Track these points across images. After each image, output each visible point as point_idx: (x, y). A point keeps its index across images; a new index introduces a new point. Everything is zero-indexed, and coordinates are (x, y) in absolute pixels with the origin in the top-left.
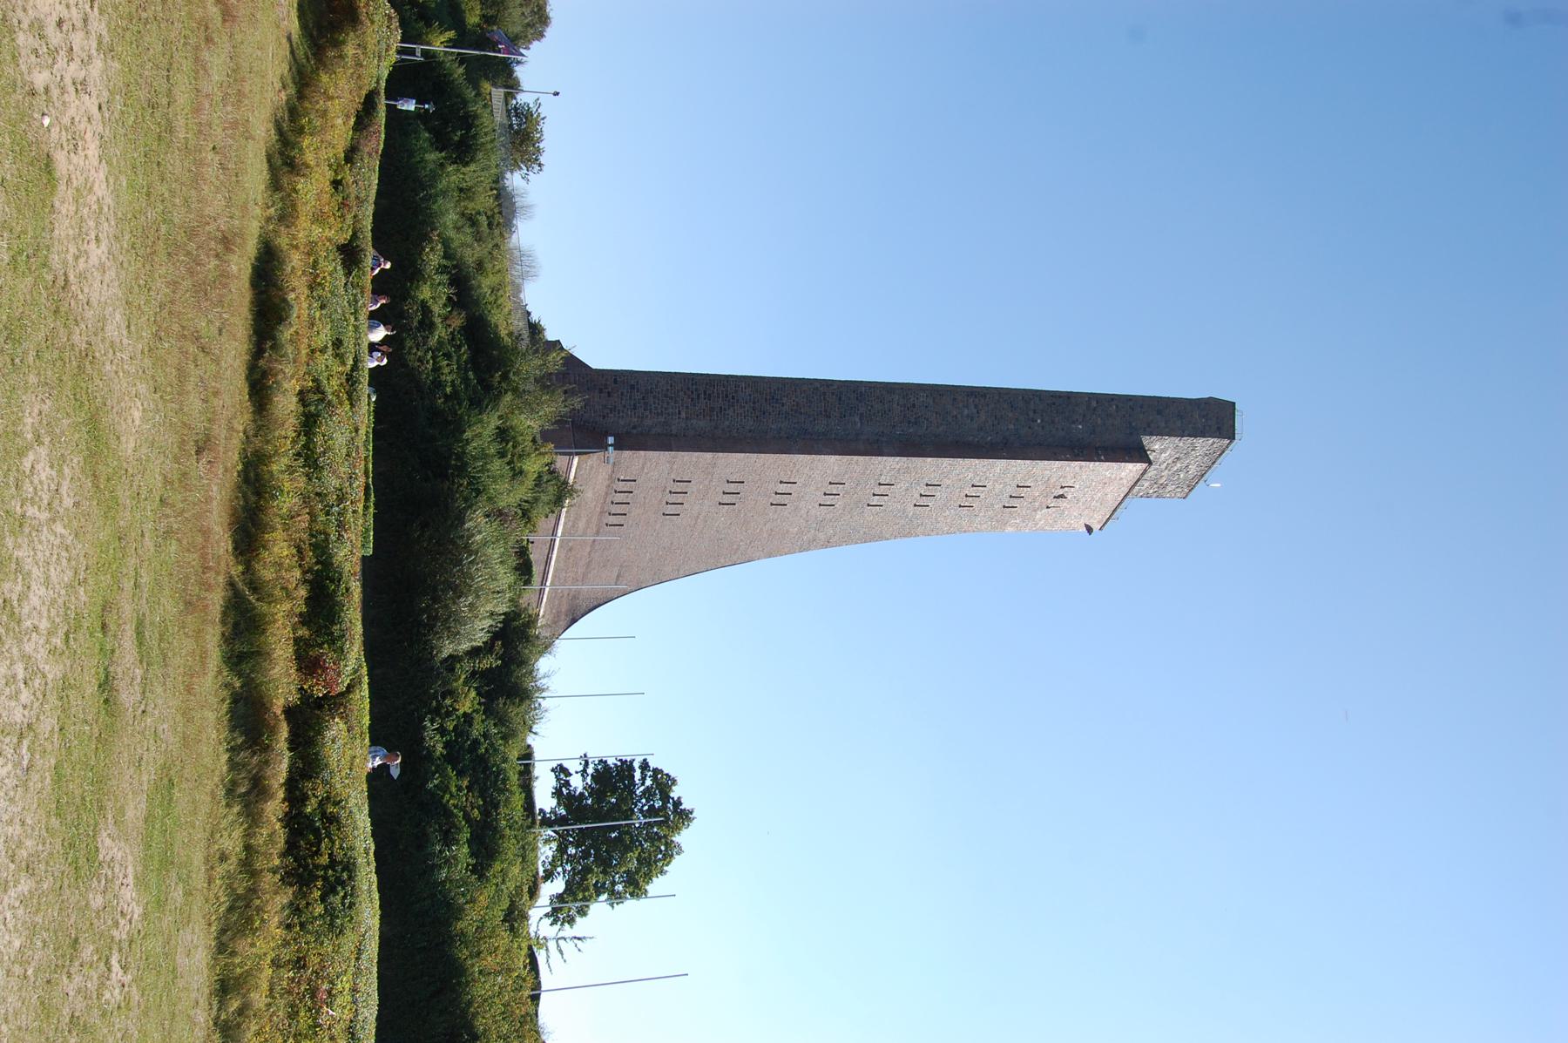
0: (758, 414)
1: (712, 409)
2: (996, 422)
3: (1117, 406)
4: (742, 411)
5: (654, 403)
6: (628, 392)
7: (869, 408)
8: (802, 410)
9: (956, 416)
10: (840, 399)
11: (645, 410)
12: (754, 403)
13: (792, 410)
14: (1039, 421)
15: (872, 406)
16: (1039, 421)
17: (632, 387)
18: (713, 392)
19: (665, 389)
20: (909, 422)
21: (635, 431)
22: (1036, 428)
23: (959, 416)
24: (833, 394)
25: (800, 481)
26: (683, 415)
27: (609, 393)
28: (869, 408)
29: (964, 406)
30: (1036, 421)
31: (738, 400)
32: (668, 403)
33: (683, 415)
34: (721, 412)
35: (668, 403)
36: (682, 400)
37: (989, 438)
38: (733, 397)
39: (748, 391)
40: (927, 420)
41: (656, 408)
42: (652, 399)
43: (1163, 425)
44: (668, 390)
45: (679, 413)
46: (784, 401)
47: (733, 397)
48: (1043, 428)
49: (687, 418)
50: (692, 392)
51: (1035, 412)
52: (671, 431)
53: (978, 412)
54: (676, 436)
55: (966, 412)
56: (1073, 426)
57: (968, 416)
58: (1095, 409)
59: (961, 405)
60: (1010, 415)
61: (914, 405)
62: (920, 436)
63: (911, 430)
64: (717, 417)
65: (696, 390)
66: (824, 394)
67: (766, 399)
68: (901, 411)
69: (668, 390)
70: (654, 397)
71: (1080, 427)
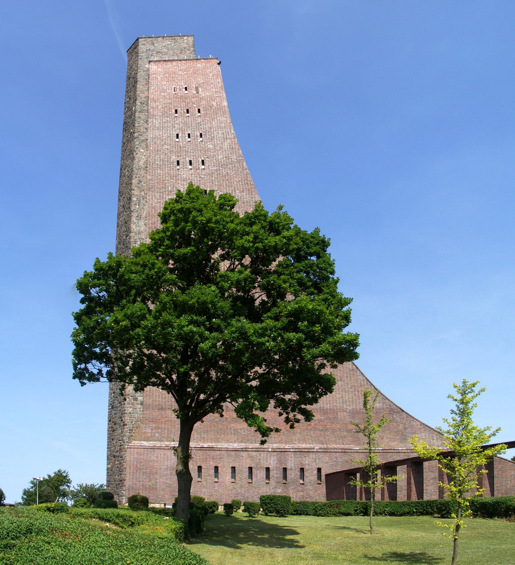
17: (112, 408)
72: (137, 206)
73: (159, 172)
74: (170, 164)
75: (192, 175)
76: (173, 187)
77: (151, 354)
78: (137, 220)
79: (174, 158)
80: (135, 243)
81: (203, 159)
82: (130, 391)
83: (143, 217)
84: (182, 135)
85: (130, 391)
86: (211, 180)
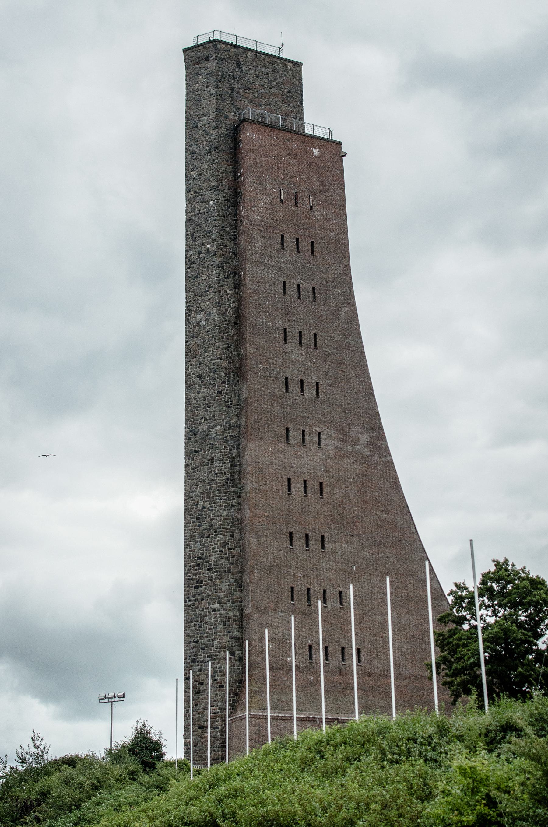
0: (212, 532)
1: (210, 579)
2: (211, 290)
3: (192, 170)
4: (210, 548)
5: (207, 637)
6: (198, 665)
7: (203, 420)
8: (208, 487)
9: (207, 332)
10: (196, 452)
11: (213, 646)
12: (203, 537)
13: (208, 498)
14: (208, 246)
15: (202, 418)
16: (208, 246)
17: (193, 661)
18: (196, 579)
19: (193, 628)
20: (214, 378)
21: (238, 653)
22: (214, 248)
23: (208, 329)
24: (193, 459)
25: (287, 475)
26: (216, 606)
27: (199, 684)
28: (203, 420)
29: (198, 326)
30: (208, 249)
31: (202, 554)
32: (206, 623)
33: (216, 606)
34: (212, 569)
35: (206, 623)
36: (203, 609)
37: (229, 292)
38: (199, 558)
39: (193, 544)
40: (211, 360)
41: (212, 634)
42: (203, 640)
43: (206, 118)
44: (195, 625)
45: (214, 610)
46: (200, 507)
47: (199, 558)
48: (214, 240)
49: (219, 602)
50: (195, 600)
51: (200, 253)
52: (235, 616)
53: (203, 310)
54: (242, 610)
55: (203, 323)
56: (211, 209)
57: (206, 320)
58: (196, 192)
59: (197, 329)
60: (204, 277)
61: (200, 376)
62: (230, 363)
63: (223, 374)
64: (216, 572)
65: (194, 596)
66: (193, 468)
67: (200, 525)
68: (205, 388)
69: (195, 625)
70: (201, 637)
71: (211, 203)
72: (226, 386)
73: (262, 343)
74: (276, 333)
75: (302, 355)
76: (280, 372)
77: (461, 641)
78: (226, 406)
79: (280, 324)
80: (225, 442)
81: (315, 332)
82: (226, 642)
83: (234, 403)
84: (290, 285)
85: (226, 642)
86: (324, 368)
